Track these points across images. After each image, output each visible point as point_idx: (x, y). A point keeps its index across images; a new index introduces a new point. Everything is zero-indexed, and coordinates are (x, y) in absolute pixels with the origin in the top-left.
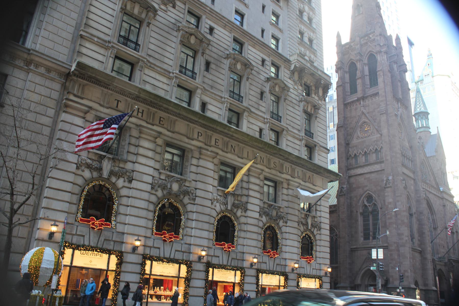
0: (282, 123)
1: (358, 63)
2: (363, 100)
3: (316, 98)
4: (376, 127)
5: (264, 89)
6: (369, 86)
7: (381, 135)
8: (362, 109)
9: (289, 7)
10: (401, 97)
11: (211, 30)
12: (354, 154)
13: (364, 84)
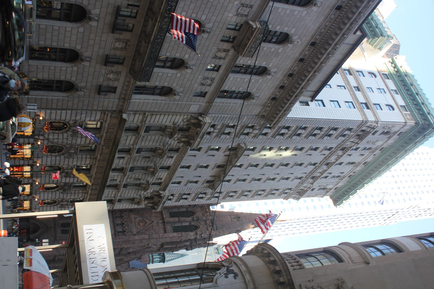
0: (122, 188)
1: (191, 219)
2: (163, 222)
3: (146, 203)
4: (141, 231)
5: (141, 180)
6: (173, 226)
7: (135, 235)
8: (156, 221)
9: (205, 188)
10: (165, 247)
11: (172, 157)
12: (123, 215)
13: (175, 222)
